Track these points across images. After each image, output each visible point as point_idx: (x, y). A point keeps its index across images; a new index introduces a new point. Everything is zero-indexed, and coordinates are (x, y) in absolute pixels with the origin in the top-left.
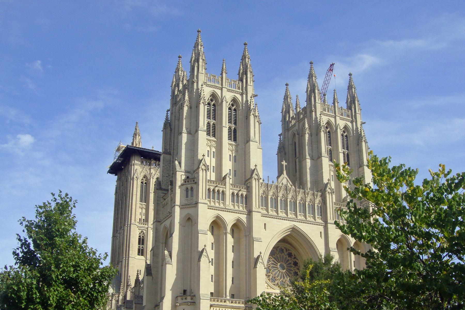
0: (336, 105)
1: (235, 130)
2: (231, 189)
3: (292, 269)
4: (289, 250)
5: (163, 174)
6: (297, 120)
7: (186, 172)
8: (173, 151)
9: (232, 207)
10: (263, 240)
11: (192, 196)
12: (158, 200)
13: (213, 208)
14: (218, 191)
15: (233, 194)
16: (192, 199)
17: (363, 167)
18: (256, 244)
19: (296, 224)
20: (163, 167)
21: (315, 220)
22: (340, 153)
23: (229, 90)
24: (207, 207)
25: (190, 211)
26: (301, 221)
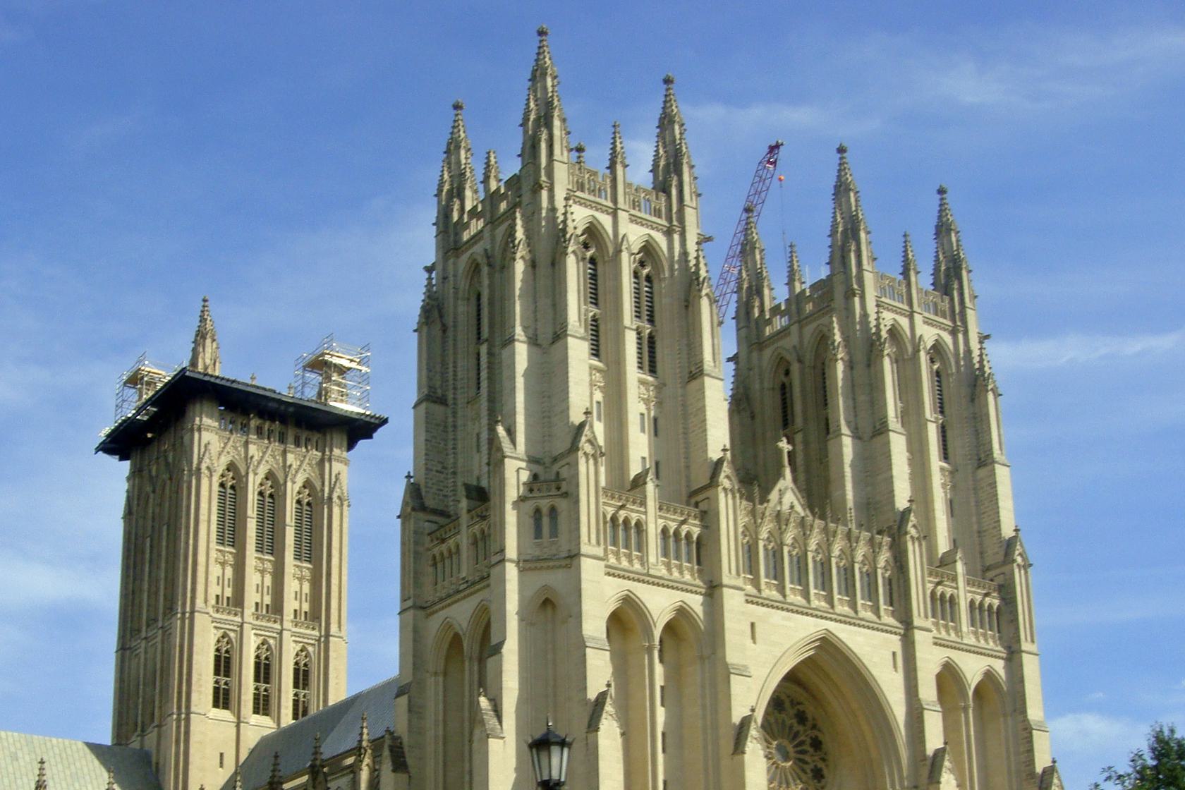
0: (913, 279)
1: (652, 340)
2: (661, 517)
3: (807, 758)
4: (799, 703)
5: (426, 464)
6: (795, 319)
7: (532, 460)
8: (454, 394)
9: (663, 572)
10: (753, 671)
11: (554, 532)
12: (416, 543)
13: (617, 572)
14: (626, 521)
15: (665, 531)
16: (553, 543)
17: (989, 468)
18: (737, 683)
20: (426, 440)
21: (879, 617)
22: (929, 423)
23: (633, 218)
24: (603, 570)
25: (555, 579)
26: (844, 620)
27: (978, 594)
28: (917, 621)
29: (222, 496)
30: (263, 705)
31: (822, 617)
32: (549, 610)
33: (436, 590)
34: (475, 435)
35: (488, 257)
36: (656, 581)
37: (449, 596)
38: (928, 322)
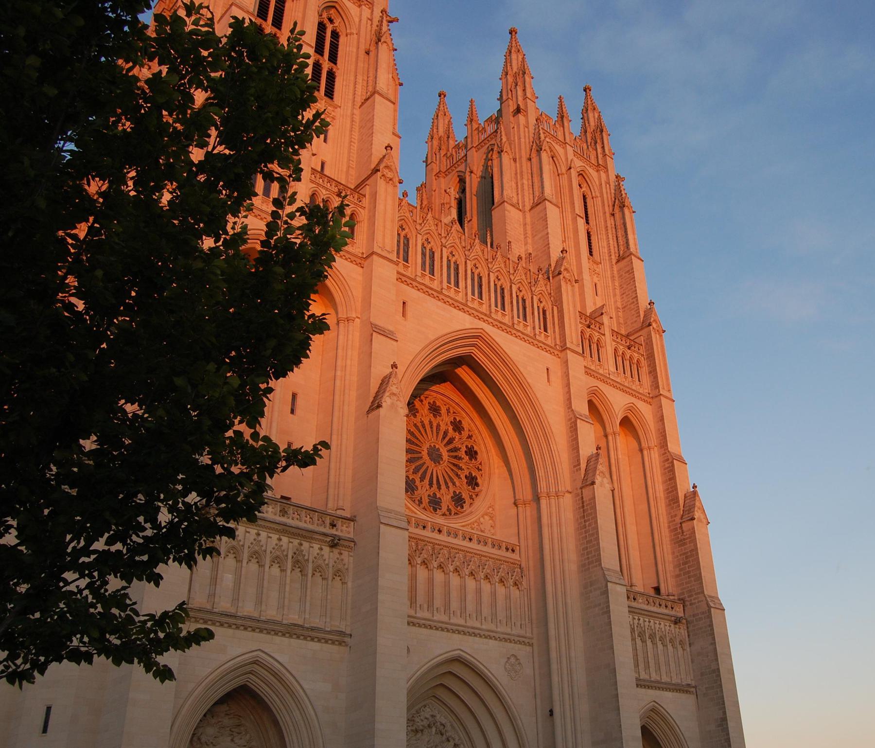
19: (488, 328)
26: (500, 326)
27: (622, 345)
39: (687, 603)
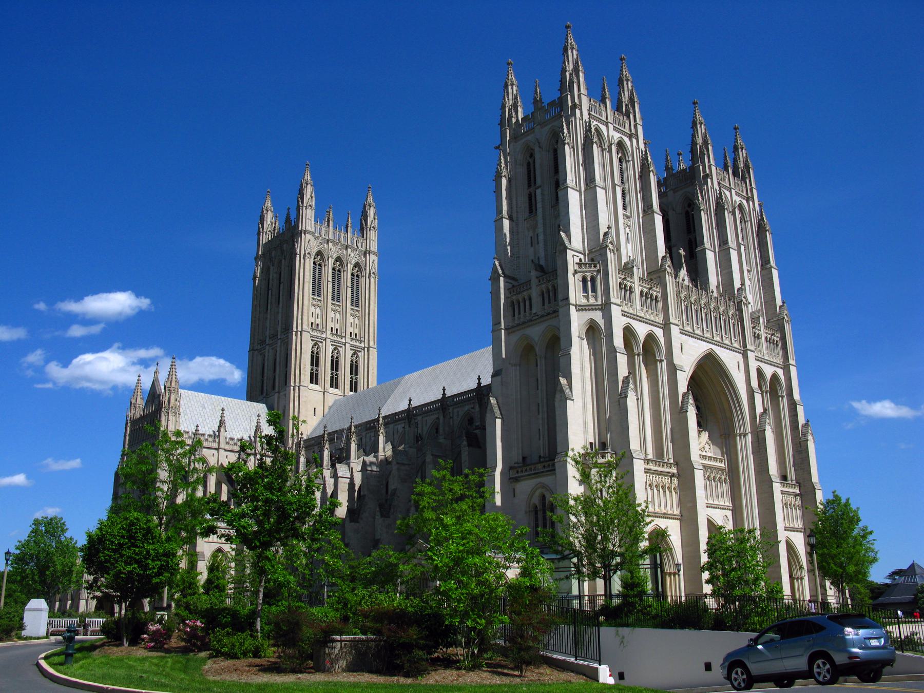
2: (640, 285)
9: (642, 315)
11: (594, 290)
15: (642, 292)
24: (620, 313)
28: (749, 347)
29: (314, 269)
30: (334, 383)
31: (709, 342)
32: (591, 333)
33: (514, 320)
34: (529, 239)
35: (539, 143)
36: (640, 319)
37: (524, 323)
38: (737, 194)
39: (802, 485)
